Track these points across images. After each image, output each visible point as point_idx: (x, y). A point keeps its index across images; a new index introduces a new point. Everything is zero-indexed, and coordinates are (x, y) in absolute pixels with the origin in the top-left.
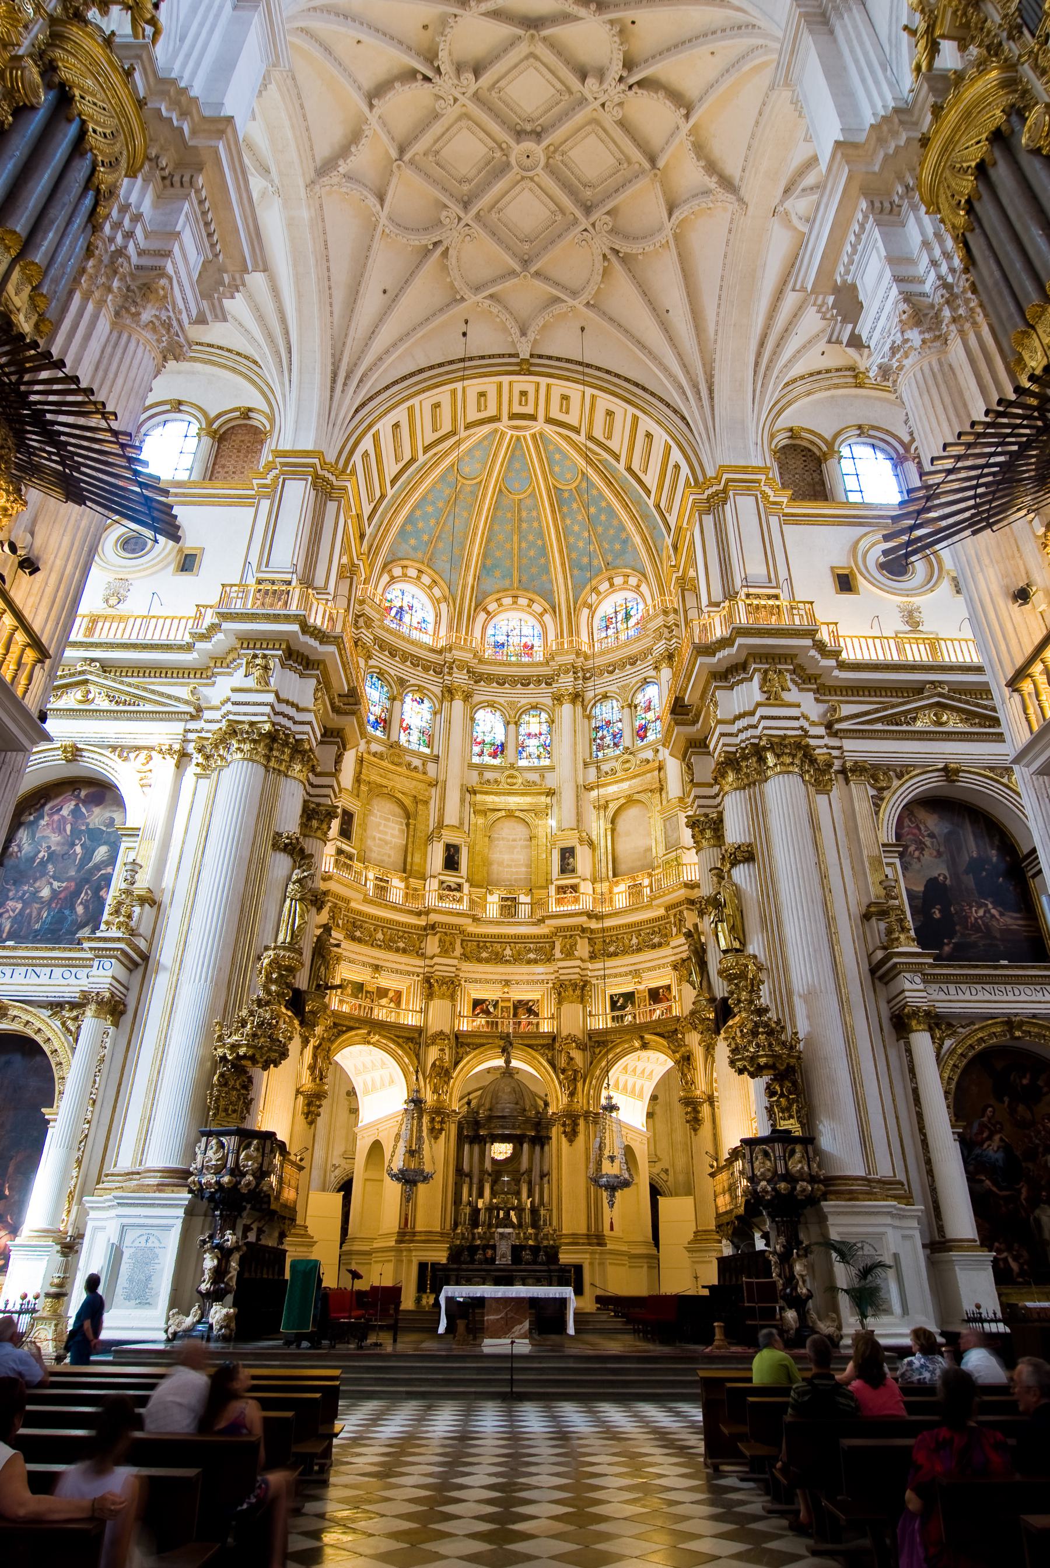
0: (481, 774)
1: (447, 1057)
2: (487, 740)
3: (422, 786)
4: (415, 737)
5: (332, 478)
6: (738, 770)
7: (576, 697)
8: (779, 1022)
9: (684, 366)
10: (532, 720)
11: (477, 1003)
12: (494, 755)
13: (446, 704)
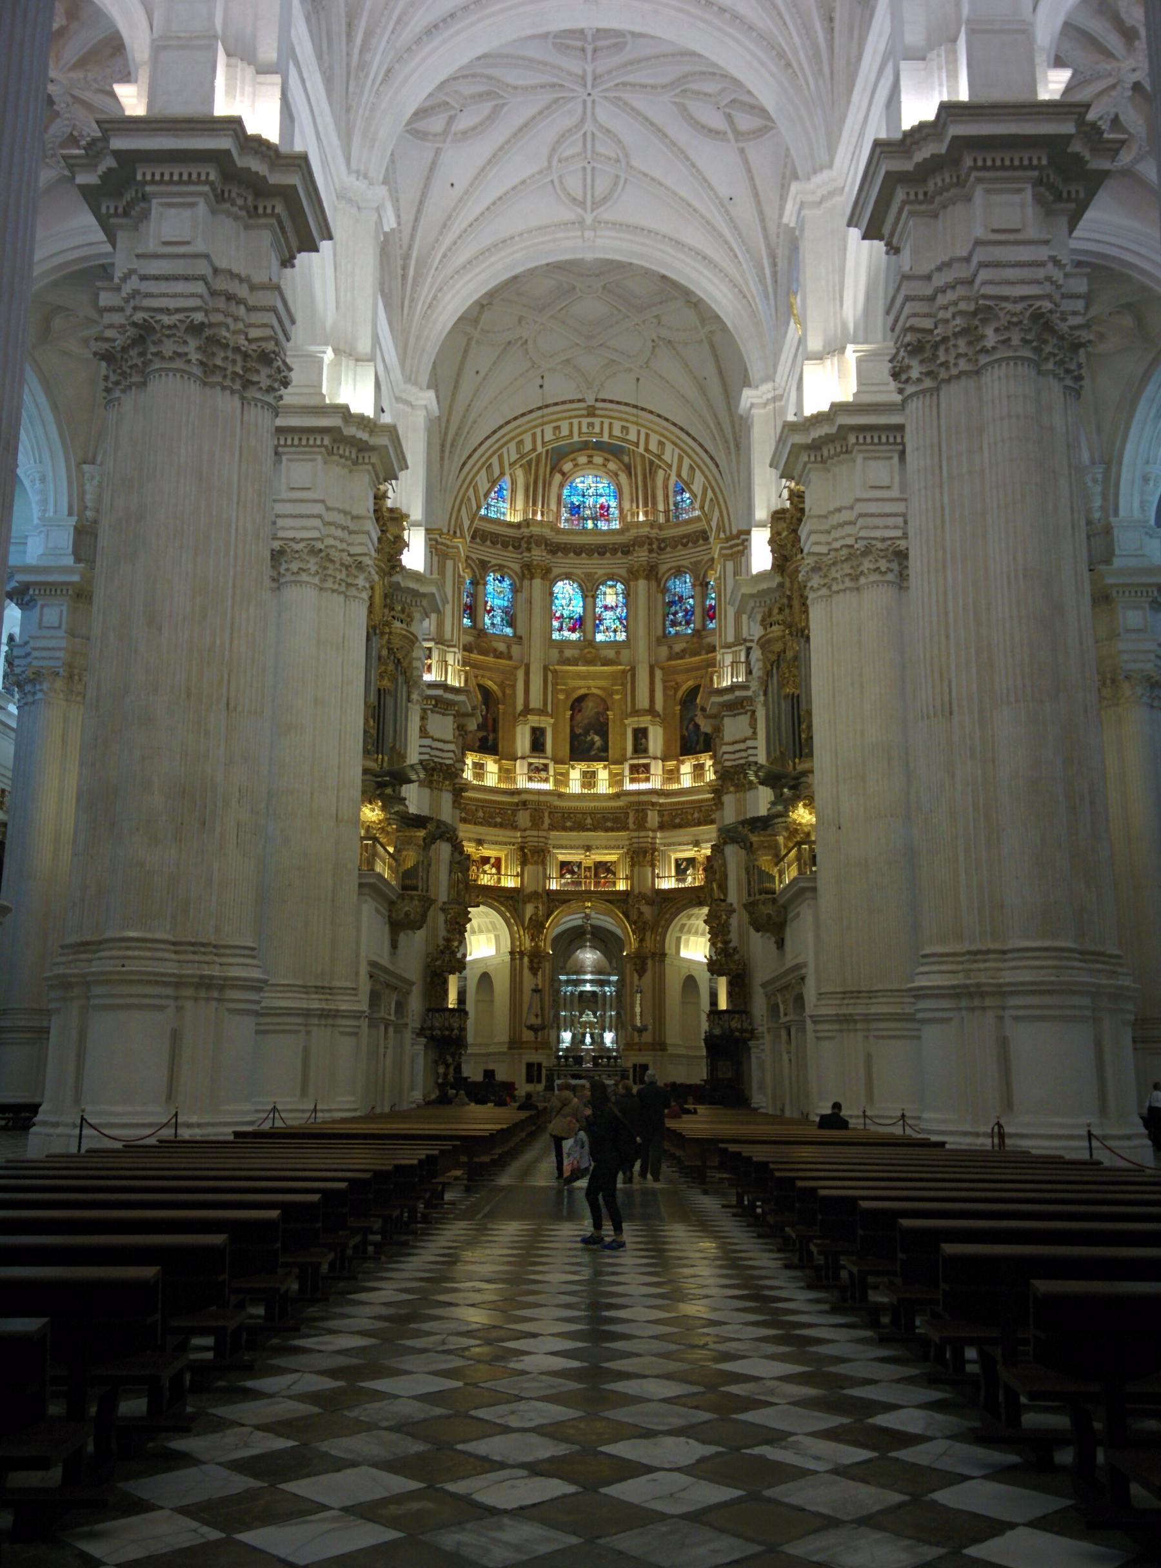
0: (561, 652)
1: (540, 913)
2: (566, 613)
4: (497, 620)
5: (448, 542)
6: (732, 780)
7: (652, 573)
8: (735, 949)
10: (609, 591)
11: (563, 865)
12: (573, 630)
13: (526, 583)
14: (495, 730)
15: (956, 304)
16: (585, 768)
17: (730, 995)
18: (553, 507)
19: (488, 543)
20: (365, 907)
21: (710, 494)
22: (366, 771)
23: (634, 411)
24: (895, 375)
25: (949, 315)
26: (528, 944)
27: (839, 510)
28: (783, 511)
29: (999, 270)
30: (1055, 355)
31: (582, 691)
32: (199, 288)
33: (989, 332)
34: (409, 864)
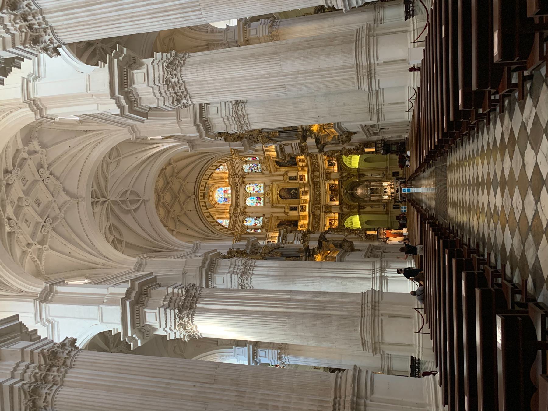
3: (273, 219)
4: (258, 222)
7: (243, 177)
8: (356, 147)
9: (200, 158)
10: (249, 189)
11: (331, 200)
12: (260, 200)
14: (291, 222)
15: (165, 91)
16: (301, 195)
17: (370, 147)
18: (224, 206)
19: (236, 225)
20: (347, 259)
21: (220, 160)
22: (306, 260)
23: (197, 183)
24: (186, 107)
25: (168, 92)
26: (356, 210)
27: (224, 122)
28: (225, 138)
29: (155, 78)
30: (179, 61)
31: (278, 196)
32: (168, 311)
33: (173, 80)
34: (333, 246)
